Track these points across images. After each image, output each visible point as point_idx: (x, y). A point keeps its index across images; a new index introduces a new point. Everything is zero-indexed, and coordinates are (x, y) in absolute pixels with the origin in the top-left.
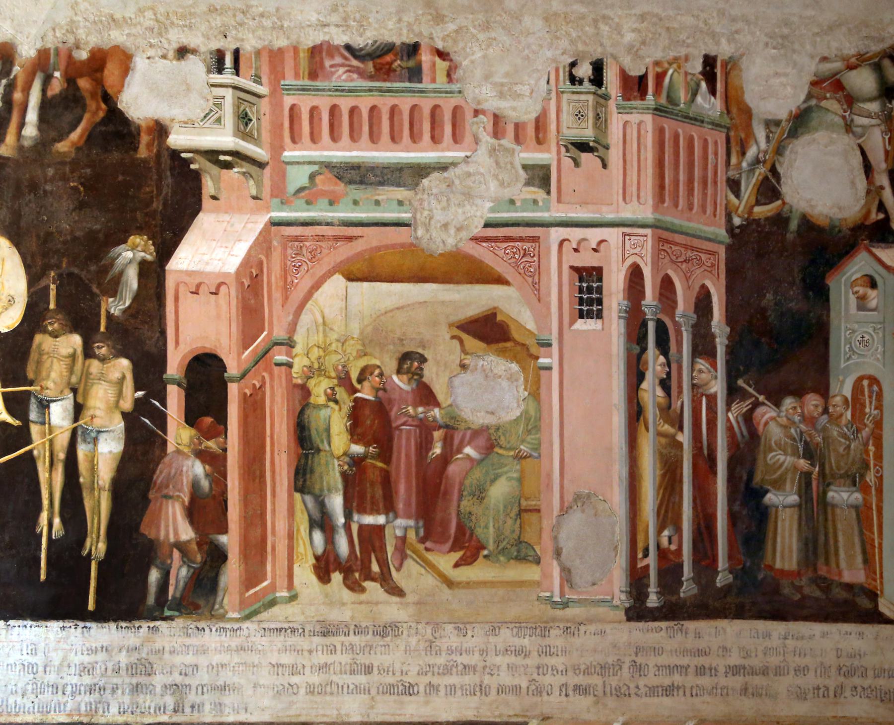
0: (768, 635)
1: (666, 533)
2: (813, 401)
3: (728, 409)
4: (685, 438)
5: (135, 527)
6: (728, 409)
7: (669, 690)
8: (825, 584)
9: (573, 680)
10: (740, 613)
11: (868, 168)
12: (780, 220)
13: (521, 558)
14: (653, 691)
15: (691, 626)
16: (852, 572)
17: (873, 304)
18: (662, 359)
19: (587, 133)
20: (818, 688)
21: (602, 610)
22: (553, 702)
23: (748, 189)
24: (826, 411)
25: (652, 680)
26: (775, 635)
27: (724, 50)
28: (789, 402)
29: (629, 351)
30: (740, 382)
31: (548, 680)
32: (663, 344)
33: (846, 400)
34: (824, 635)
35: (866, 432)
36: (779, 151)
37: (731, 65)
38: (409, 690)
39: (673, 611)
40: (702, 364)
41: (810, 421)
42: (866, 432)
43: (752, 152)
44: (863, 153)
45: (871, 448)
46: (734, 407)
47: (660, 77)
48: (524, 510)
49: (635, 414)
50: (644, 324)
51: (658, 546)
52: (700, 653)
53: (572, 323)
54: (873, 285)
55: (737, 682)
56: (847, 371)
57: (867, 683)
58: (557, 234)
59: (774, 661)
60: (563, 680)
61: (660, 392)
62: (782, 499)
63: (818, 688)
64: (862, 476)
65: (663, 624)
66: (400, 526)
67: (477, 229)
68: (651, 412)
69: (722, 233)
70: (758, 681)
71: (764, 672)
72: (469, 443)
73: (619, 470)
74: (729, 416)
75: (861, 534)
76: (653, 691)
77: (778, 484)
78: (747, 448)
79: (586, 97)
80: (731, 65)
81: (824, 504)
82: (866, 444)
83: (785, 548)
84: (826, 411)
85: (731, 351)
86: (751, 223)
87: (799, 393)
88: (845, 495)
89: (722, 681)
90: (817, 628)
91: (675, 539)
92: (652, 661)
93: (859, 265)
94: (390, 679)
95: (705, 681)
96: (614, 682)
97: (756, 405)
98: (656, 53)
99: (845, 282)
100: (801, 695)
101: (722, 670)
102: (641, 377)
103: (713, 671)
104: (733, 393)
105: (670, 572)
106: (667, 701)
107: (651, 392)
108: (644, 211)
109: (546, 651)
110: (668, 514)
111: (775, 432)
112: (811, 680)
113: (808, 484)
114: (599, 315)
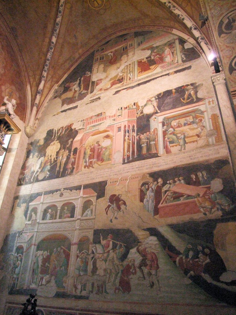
0: (142, 162)
1: (128, 153)
2: (148, 133)
3: (137, 137)
4: (131, 142)
5: (66, 167)
6: (137, 137)
7: (128, 172)
8: (150, 154)
9: (115, 173)
10: (138, 160)
11: (154, 107)
12: (143, 115)
13: (109, 160)
14: (125, 173)
15: (131, 163)
16: (154, 151)
17: (156, 120)
18: (128, 134)
19: (120, 114)
20: (149, 167)
21: (119, 164)
22: (112, 177)
23: (139, 113)
24: (150, 134)
25: (125, 171)
26: (143, 162)
27: (136, 102)
28: (145, 134)
29: (124, 134)
30: (138, 133)
31: (111, 174)
32: (128, 132)
33: (152, 132)
34: (150, 160)
35: (155, 135)
36: (143, 108)
37: (137, 103)
38: (94, 179)
39: (129, 162)
40: (133, 133)
41: (148, 135)
42: (155, 135)
43: (139, 110)
44: (153, 106)
45: (156, 136)
46: (137, 136)
47: (128, 107)
48: (110, 155)
49: (124, 140)
50: (126, 131)
51: (127, 155)
52: (133, 166)
53: (117, 133)
54: (156, 118)
55: (137, 169)
56: (153, 128)
57: (156, 165)
58: (116, 125)
59: (143, 165)
60: (113, 174)
61: (128, 137)
62: (144, 146)
63: (149, 167)
64: (155, 140)
65: (127, 164)
66: (95, 160)
67: (107, 127)
68: (126, 140)
69: (136, 119)
70: (140, 168)
71: (141, 167)
72: (104, 149)
73: (122, 147)
74: (137, 138)
75: (155, 147)
76: (125, 173)
77: (144, 144)
78: (139, 141)
79: (120, 111)
80: (137, 103)
81: (150, 144)
82: (155, 136)
83: (144, 151)
84: (150, 134)
85: (137, 131)
86: (140, 117)
87: (146, 133)
88: (153, 143)
89: (135, 169)
90: (149, 160)
91: (129, 153)
92: (126, 169)
93: (154, 117)
94: (91, 178)
95: (133, 170)
96: (120, 172)
97: (141, 135)
98: (129, 104)
99: (152, 120)
100: (147, 169)
101: (135, 168)
102: (125, 136)
103: (134, 168)
104: (137, 135)
105: (128, 157)
106: (127, 174)
107: (127, 137)
108: (127, 120)
109: (111, 171)
110: (128, 151)
111: (143, 138)
112: (148, 167)
113: (148, 143)
114: (120, 131)
